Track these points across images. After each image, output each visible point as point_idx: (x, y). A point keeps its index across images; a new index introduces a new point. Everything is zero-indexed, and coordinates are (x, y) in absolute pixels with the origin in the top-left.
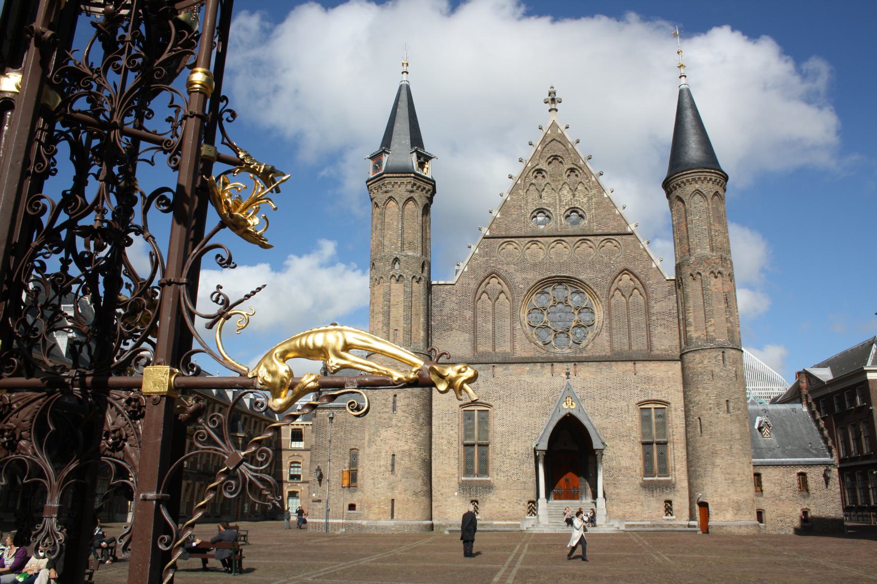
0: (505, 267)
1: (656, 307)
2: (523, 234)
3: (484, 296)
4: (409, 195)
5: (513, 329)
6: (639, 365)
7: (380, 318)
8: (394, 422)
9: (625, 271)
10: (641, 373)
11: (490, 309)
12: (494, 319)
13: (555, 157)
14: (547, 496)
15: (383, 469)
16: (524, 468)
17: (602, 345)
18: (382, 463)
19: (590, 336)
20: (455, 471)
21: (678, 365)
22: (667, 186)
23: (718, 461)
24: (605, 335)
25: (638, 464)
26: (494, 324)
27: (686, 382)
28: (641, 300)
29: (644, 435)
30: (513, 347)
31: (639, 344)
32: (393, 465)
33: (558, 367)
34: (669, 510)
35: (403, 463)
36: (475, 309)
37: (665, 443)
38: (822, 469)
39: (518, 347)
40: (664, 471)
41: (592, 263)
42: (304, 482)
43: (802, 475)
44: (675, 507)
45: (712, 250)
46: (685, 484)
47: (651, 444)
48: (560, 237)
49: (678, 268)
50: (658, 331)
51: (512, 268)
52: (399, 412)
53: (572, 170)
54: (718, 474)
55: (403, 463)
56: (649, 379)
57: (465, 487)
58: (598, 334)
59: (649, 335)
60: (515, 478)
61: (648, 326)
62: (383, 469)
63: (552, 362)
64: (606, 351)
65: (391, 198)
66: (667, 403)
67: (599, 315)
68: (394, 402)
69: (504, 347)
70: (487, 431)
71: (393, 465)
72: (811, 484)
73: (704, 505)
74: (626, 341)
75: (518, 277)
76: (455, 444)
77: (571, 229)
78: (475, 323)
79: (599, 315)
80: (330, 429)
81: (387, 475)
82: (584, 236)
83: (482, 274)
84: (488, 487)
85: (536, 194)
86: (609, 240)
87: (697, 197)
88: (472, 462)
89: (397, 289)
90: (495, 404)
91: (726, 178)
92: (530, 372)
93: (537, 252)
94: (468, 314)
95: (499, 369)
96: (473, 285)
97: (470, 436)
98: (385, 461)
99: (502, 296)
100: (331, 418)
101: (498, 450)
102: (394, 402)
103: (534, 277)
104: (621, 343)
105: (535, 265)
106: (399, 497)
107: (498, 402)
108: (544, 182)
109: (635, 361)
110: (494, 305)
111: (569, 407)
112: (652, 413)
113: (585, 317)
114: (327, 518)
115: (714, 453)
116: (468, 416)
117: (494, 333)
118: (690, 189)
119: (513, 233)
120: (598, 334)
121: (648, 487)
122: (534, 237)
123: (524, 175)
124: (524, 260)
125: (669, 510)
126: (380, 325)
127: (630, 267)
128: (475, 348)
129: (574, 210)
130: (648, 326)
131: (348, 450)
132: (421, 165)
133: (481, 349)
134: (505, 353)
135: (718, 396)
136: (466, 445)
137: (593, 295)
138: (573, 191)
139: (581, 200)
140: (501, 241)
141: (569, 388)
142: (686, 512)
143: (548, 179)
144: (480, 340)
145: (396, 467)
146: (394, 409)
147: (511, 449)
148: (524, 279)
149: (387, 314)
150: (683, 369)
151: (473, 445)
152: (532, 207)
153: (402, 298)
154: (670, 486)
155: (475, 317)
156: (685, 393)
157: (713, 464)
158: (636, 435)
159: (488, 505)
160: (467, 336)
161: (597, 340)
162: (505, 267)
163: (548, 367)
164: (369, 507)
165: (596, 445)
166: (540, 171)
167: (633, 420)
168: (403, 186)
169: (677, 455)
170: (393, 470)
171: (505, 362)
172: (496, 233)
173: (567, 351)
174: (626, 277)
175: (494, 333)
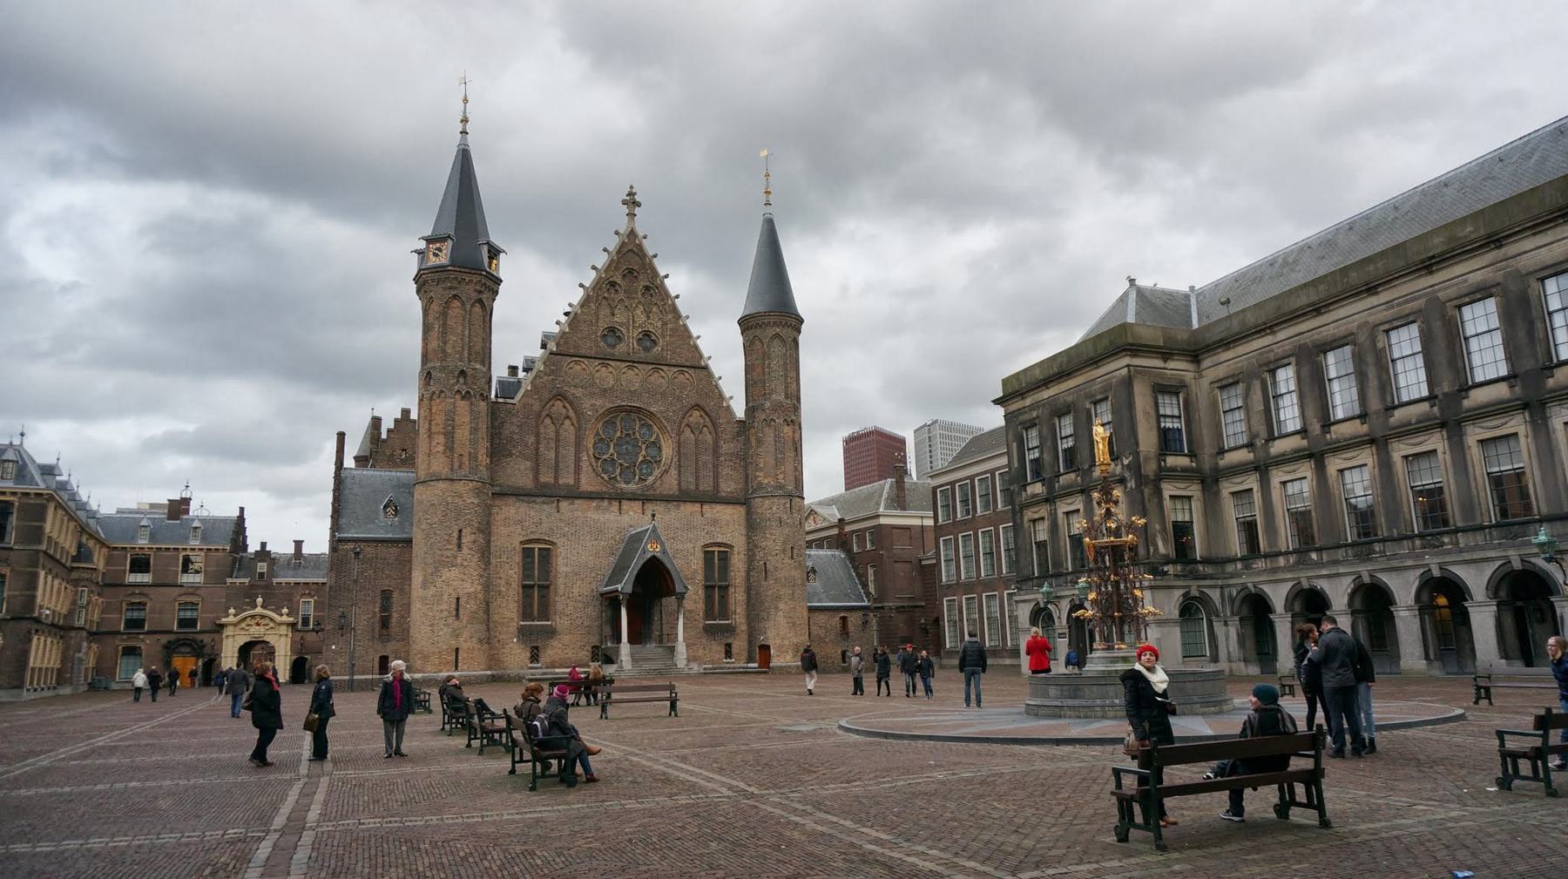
0: (573, 390)
1: (725, 448)
2: (593, 354)
3: (548, 421)
4: (475, 296)
5: (578, 460)
6: (706, 507)
7: (441, 439)
8: (459, 561)
9: (697, 406)
10: (708, 515)
11: (552, 435)
12: (557, 447)
13: (631, 271)
14: (631, 641)
15: (445, 614)
16: (589, 610)
17: (671, 484)
18: (444, 607)
19: (657, 472)
20: (514, 615)
21: (741, 510)
22: (740, 322)
23: (781, 606)
24: (673, 472)
25: (701, 606)
26: (557, 453)
27: (752, 526)
28: (709, 438)
29: (707, 577)
30: (578, 480)
31: (706, 485)
32: (457, 610)
33: (626, 505)
34: (728, 654)
35: (469, 607)
36: (537, 435)
37: (727, 587)
38: (860, 614)
39: (583, 480)
40: (724, 613)
41: (663, 394)
42: (149, 633)
43: (844, 619)
44: (734, 650)
45: (787, 397)
46: (744, 627)
47: (713, 587)
48: (632, 363)
49: (750, 410)
50: (725, 471)
51: (579, 392)
52: (465, 550)
53: (647, 288)
54: (781, 618)
55: (469, 607)
56: (715, 522)
57: (524, 633)
58: (666, 471)
59: (716, 477)
60: (579, 622)
61: (715, 467)
62: (445, 614)
63: (620, 498)
64: (674, 490)
65: (455, 296)
66: (731, 547)
67: (668, 451)
68: (460, 538)
69: (567, 479)
70: (548, 572)
71: (457, 610)
72: (851, 627)
73: (765, 649)
74: (692, 480)
75: (587, 404)
76: (514, 585)
77: (642, 355)
78: (537, 449)
79: (668, 451)
80: (356, 567)
81: (450, 620)
82: (657, 364)
83: (547, 395)
84: (551, 633)
85: (608, 311)
86: (682, 372)
87: (776, 342)
88: (531, 606)
89: (463, 405)
90: (560, 541)
91: (802, 321)
92: (598, 508)
93: (606, 376)
94: (531, 439)
95: (564, 504)
96: (536, 408)
97: (531, 577)
98: (447, 605)
99: (567, 422)
100: (357, 554)
101: (561, 592)
102: (460, 538)
103: (603, 404)
104: (689, 481)
105: (605, 391)
106: (464, 646)
107: (563, 540)
108: (618, 297)
109: (702, 503)
110: (557, 432)
111: (653, 549)
112: (716, 559)
113: (653, 452)
114: (353, 674)
115: (778, 598)
116: (528, 553)
117: (557, 463)
118: (771, 331)
119: (583, 352)
120: (666, 471)
121: (710, 631)
122: (604, 359)
123: (597, 285)
124: (593, 384)
125: (728, 654)
126: (441, 448)
127: (702, 403)
128: (536, 478)
129: (647, 334)
130: (715, 467)
131: (378, 592)
132: (491, 258)
133: (542, 479)
134: (567, 485)
135: (784, 542)
136: (524, 587)
137: (662, 429)
138: (648, 313)
139: (655, 325)
140: (569, 359)
141: (654, 530)
142: (745, 654)
143: (622, 295)
144: (543, 469)
145: (461, 611)
146: (459, 546)
147: (576, 591)
148: (593, 405)
149: (450, 435)
150: (749, 513)
151: (532, 587)
152: (603, 325)
153: (467, 419)
154: (730, 630)
155: (538, 443)
156: (749, 537)
157: (777, 608)
158: (700, 577)
159: (550, 652)
160: (528, 464)
161: (665, 478)
162: (573, 390)
163: (616, 504)
164: (425, 658)
165: (679, 588)
166: (613, 284)
167: (697, 562)
168: (471, 287)
169: (737, 597)
170: (457, 615)
171: (574, 495)
172: (563, 349)
173: (632, 487)
174: (696, 413)
175: (557, 463)
